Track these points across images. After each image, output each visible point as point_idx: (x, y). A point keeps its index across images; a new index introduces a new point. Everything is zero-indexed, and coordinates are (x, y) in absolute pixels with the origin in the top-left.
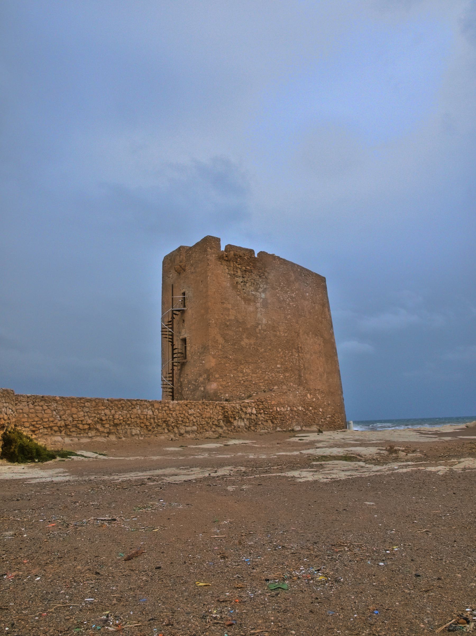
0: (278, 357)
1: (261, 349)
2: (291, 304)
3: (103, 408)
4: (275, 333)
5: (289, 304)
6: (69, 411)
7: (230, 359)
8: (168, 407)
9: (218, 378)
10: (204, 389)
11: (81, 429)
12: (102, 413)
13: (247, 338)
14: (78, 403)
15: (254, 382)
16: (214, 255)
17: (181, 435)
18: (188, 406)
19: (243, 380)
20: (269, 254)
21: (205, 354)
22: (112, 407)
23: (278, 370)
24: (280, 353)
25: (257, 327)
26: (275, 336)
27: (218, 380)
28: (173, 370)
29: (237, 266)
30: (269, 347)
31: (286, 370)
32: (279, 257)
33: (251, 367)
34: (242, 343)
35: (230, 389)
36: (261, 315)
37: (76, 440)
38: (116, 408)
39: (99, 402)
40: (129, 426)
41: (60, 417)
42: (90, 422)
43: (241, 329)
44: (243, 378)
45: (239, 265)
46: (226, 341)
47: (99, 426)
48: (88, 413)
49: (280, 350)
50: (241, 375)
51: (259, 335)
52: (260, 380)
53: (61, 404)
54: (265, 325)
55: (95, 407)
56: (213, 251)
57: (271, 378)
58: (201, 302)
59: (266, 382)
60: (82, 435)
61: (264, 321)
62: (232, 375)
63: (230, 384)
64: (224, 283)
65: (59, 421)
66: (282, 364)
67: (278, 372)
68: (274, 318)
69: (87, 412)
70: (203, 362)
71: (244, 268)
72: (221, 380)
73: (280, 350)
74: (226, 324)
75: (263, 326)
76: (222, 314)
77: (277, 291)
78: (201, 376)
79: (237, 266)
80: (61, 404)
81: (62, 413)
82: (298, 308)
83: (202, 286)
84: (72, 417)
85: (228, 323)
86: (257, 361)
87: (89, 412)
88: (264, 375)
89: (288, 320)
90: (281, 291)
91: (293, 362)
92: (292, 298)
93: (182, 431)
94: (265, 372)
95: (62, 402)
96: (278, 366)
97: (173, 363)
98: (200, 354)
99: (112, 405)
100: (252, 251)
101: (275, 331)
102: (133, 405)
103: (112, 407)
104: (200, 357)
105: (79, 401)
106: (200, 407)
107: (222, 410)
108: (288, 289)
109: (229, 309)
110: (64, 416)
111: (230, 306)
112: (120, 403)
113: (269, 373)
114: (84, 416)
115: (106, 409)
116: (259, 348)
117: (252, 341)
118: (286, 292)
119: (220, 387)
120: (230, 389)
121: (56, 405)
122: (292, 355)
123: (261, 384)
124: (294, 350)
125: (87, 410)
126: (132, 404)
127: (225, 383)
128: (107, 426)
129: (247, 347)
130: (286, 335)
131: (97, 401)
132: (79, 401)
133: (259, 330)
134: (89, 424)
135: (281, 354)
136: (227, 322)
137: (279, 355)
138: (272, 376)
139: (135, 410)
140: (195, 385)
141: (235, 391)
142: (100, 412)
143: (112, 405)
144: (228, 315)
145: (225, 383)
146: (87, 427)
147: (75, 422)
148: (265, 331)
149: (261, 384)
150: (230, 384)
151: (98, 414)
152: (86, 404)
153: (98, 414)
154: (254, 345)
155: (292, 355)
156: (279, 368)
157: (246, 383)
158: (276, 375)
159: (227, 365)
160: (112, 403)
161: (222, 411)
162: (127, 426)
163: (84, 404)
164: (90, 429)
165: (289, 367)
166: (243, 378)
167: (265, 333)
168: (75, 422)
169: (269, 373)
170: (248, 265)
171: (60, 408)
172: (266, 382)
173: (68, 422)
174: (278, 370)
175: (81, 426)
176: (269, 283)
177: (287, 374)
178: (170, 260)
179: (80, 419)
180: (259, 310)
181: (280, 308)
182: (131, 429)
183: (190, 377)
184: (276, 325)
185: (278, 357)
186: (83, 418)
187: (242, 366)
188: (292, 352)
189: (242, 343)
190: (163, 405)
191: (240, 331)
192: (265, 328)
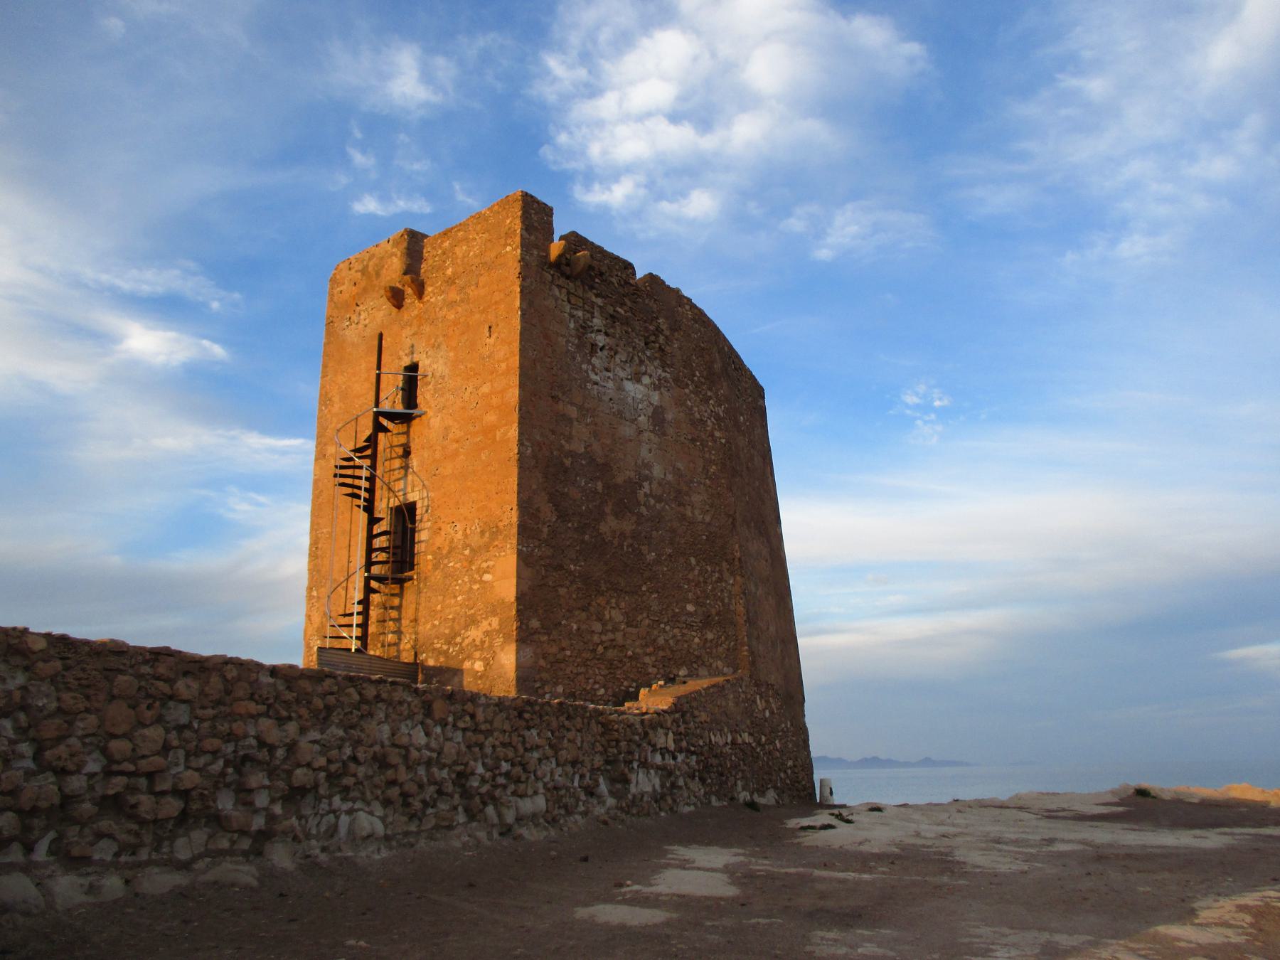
0: (688, 581)
1: (649, 552)
2: (717, 434)
3: (253, 707)
4: (681, 509)
5: (712, 435)
6: (92, 719)
7: (571, 573)
8: (473, 716)
9: (536, 632)
10: (487, 665)
11: (142, 822)
12: (246, 736)
13: (616, 515)
14: (140, 677)
15: (630, 653)
16: (535, 252)
17: (506, 831)
18: (527, 716)
19: (602, 642)
20: (668, 287)
21: (493, 551)
22: (287, 704)
23: (690, 619)
24: (693, 569)
25: (641, 486)
26: (683, 518)
27: (536, 637)
28: (365, 602)
29: (594, 299)
30: (669, 551)
31: (707, 622)
32: (689, 300)
33: (623, 605)
34: (603, 528)
35: (568, 671)
36: (650, 451)
37: (113, 884)
38: (304, 712)
39: (239, 679)
40: (344, 800)
41: (36, 757)
42: (190, 779)
43: (600, 486)
44: (604, 638)
45: (597, 296)
46: (563, 516)
47: (226, 803)
48: (187, 734)
49: (693, 560)
50: (598, 627)
51: (643, 510)
52: (647, 645)
53: (53, 679)
54: (660, 484)
55: (219, 703)
56: (533, 238)
57: (671, 642)
58: (485, 389)
59: (661, 653)
60: (144, 855)
61: (657, 471)
62: (575, 627)
63: (568, 653)
64: (560, 339)
65: (29, 774)
66: (697, 603)
67: (689, 627)
68: (679, 465)
69: (180, 728)
70: (487, 577)
71: (610, 310)
72: (545, 638)
73: (693, 560)
74: (562, 464)
75: (655, 486)
76: (553, 432)
77: (687, 391)
78: (473, 621)
79: (594, 299)
80: (53, 679)
81: (50, 729)
82: (730, 449)
83: (492, 341)
84: (104, 751)
85: (568, 462)
86: (640, 587)
87: (188, 726)
88: (656, 632)
89: (710, 479)
90: (696, 393)
91: (722, 601)
92: (718, 418)
93: (510, 817)
94: (659, 622)
95: (58, 664)
96: (690, 608)
97: (367, 580)
98: (472, 550)
99: (289, 696)
100: (628, 267)
101: (680, 504)
102: (367, 702)
103: (287, 704)
104: (471, 563)
105: (146, 669)
106: (554, 724)
107: (602, 734)
108: (709, 394)
109: (570, 421)
110: (62, 750)
111: (573, 412)
112: (320, 689)
113: (668, 628)
114: (166, 748)
115: (266, 715)
116: (644, 549)
117: (628, 526)
118: (706, 400)
119: (542, 662)
120: (568, 671)
121: (21, 679)
122: (720, 580)
123: (647, 660)
124: (724, 564)
125: (180, 714)
126: (363, 700)
127: (554, 649)
128: (261, 800)
129: (616, 542)
130: (708, 519)
131: (232, 673)
132: (146, 669)
133: (646, 495)
134: (184, 794)
135: (696, 572)
136: (566, 457)
137: (690, 576)
138: (674, 636)
139: (371, 726)
140: (446, 653)
141: (581, 678)
142: (238, 727)
143: (289, 696)
144: (569, 439)
145: (554, 649)
146: (173, 806)
147: (119, 783)
148: (659, 499)
149: (647, 660)
150: (568, 653)
151: (230, 737)
152: (180, 685)
153: (230, 737)
154: (633, 538)
155: (720, 580)
156: (690, 614)
157: (611, 654)
158: (683, 635)
159: (562, 591)
160: (289, 688)
161: (604, 741)
162: (337, 800)
163: (171, 681)
164: (183, 819)
165: (713, 611)
166: (604, 638)
167: (658, 506)
168: (119, 783)
169: (668, 628)
170: (622, 305)
171: (44, 700)
172: (661, 653)
173: (76, 783)
174: (690, 619)
175: (145, 802)
176: (669, 366)
177: (710, 636)
178: (364, 271)
179: (143, 763)
180: (646, 435)
181: (693, 440)
182: (350, 812)
183: (425, 628)
184: (685, 489)
185: (688, 581)
186: (158, 760)
187: (601, 600)
188: (720, 572)
189: (603, 528)
190: (458, 707)
191: (596, 492)
192: (659, 492)
